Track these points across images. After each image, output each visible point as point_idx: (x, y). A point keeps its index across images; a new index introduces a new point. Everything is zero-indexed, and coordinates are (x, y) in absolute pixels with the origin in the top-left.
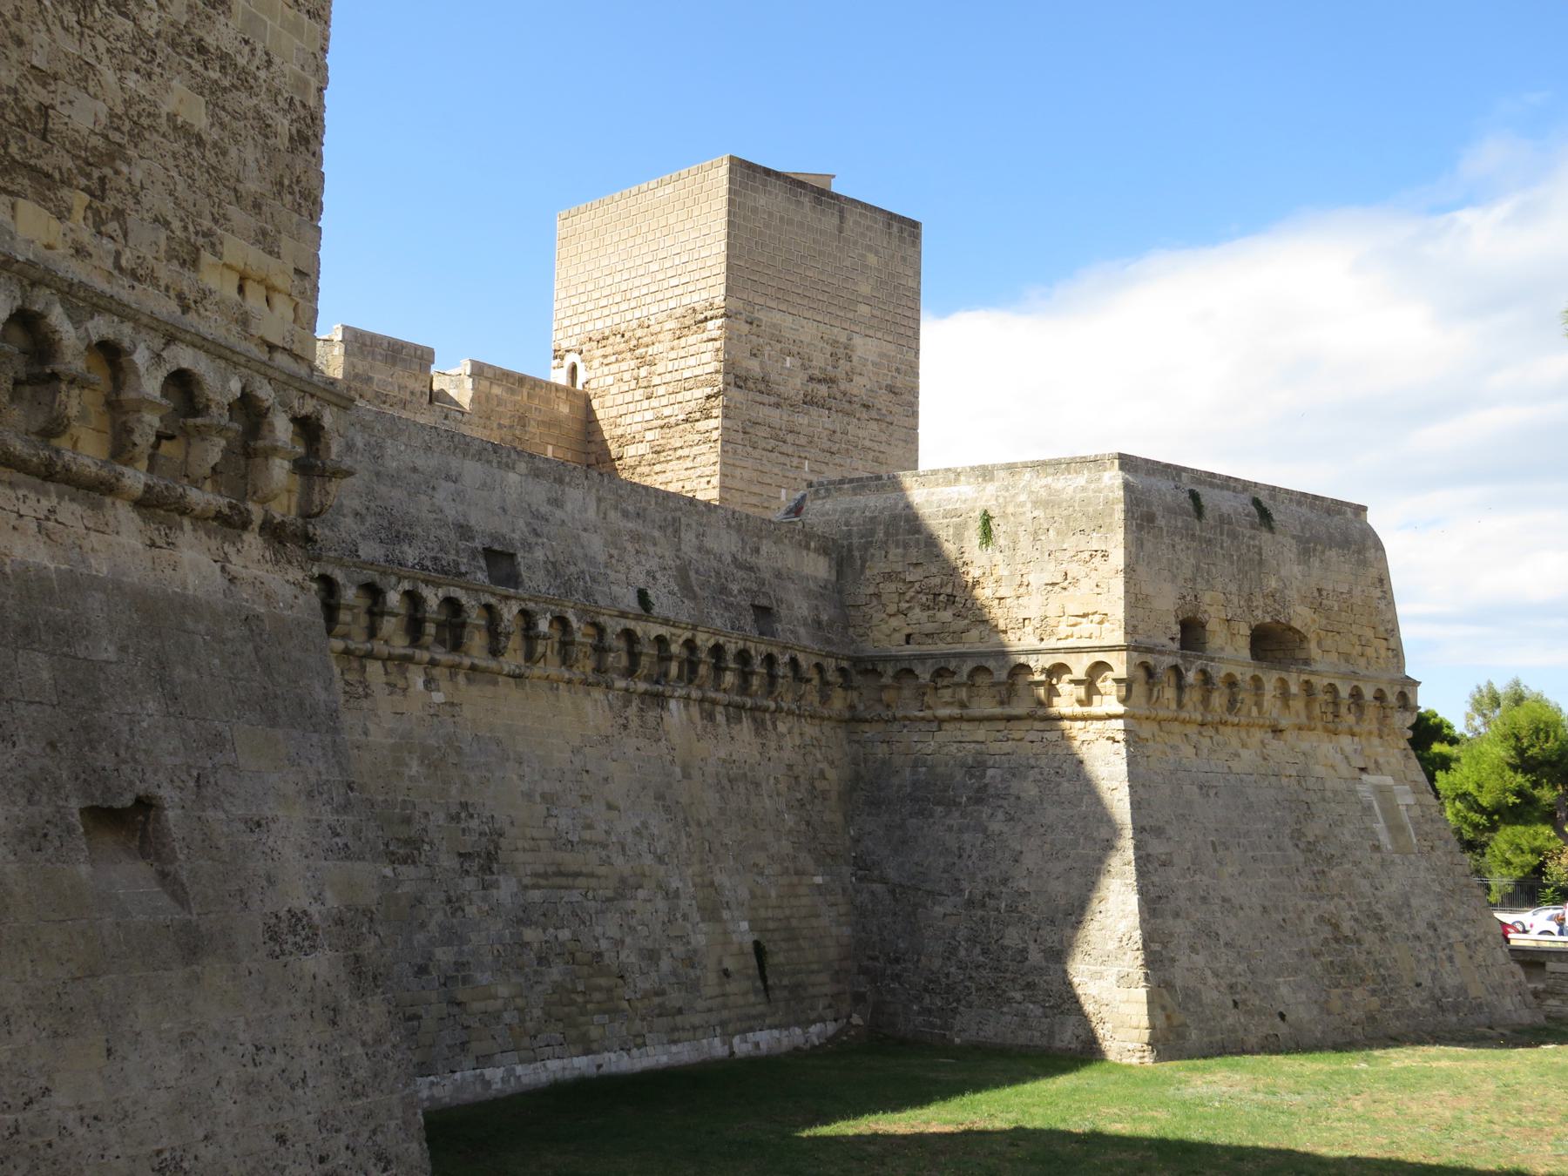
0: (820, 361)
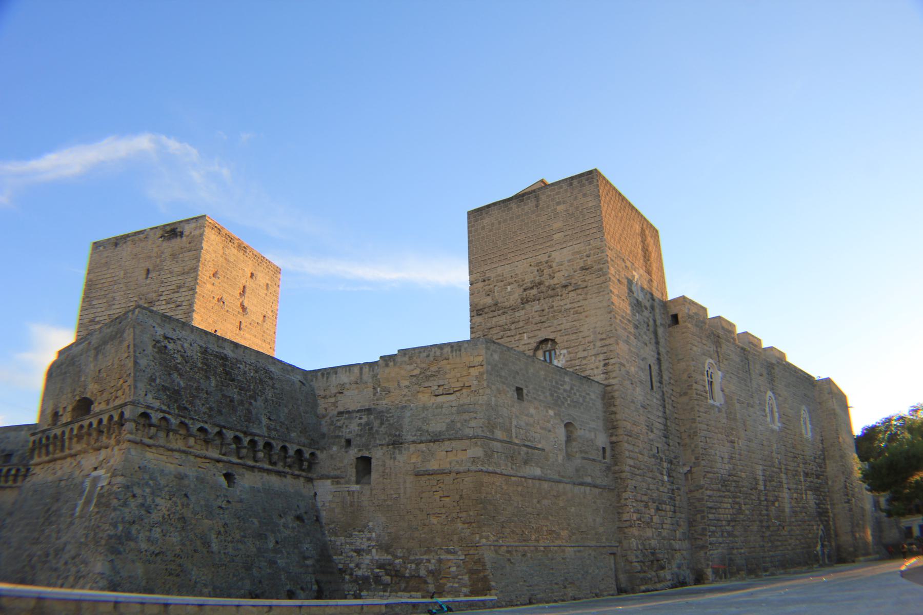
0: (529, 278)
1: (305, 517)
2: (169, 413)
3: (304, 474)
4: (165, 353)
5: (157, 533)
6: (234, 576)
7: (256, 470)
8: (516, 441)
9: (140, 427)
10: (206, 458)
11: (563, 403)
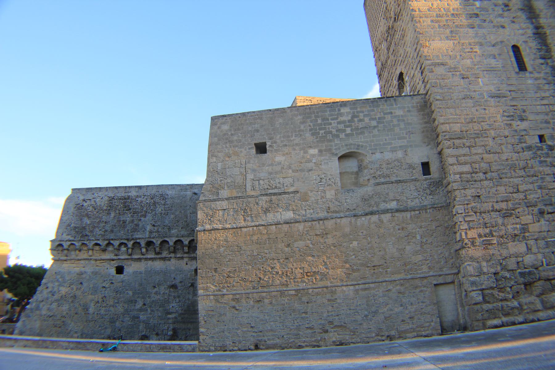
1: (179, 285)
2: (73, 241)
3: (185, 255)
4: (82, 209)
5: (54, 305)
6: (99, 327)
7: (143, 260)
8: (253, 193)
9: (60, 252)
10: (104, 260)
11: (338, 136)
